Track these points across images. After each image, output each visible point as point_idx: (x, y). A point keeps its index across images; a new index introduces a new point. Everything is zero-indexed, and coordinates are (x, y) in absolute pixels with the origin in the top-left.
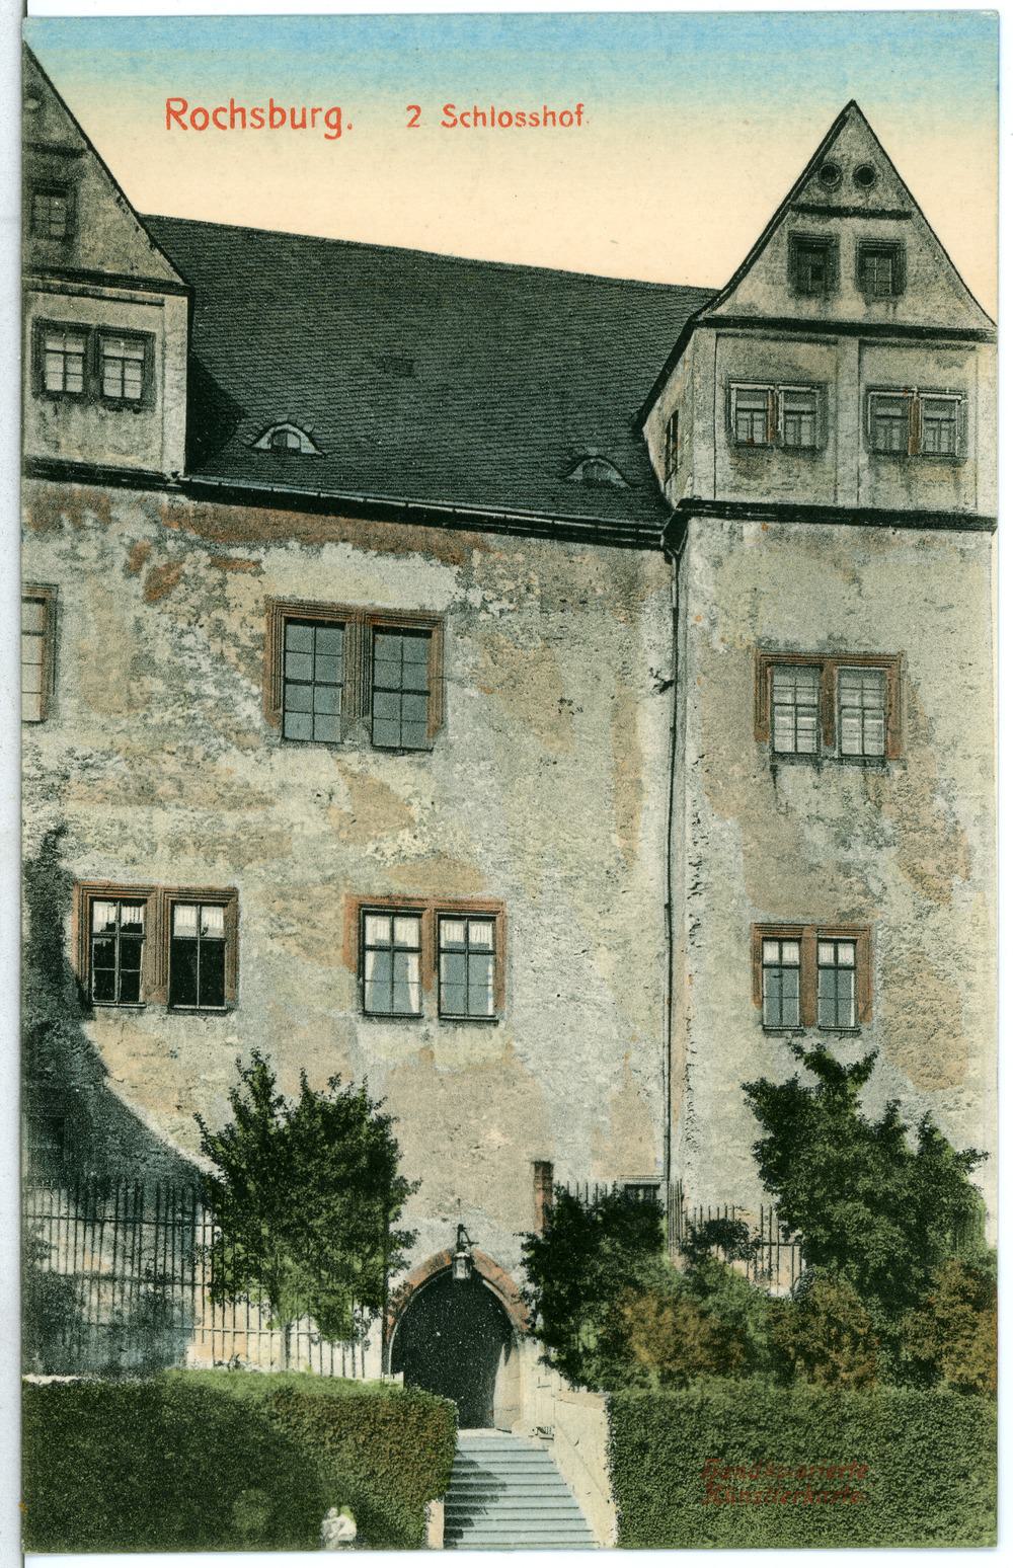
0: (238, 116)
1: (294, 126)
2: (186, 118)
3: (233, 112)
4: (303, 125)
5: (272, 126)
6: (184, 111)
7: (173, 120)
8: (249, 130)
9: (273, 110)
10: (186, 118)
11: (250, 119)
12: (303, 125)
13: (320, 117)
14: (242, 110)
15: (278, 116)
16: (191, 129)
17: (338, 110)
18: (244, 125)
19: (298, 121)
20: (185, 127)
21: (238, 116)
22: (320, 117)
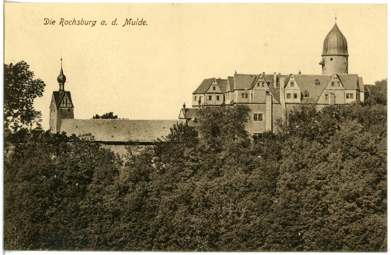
0: (75, 22)
2: (64, 23)
11: (77, 23)
13: (91, 23)
14: (75, 21)
17: (96, 22)
22: (91, 23)
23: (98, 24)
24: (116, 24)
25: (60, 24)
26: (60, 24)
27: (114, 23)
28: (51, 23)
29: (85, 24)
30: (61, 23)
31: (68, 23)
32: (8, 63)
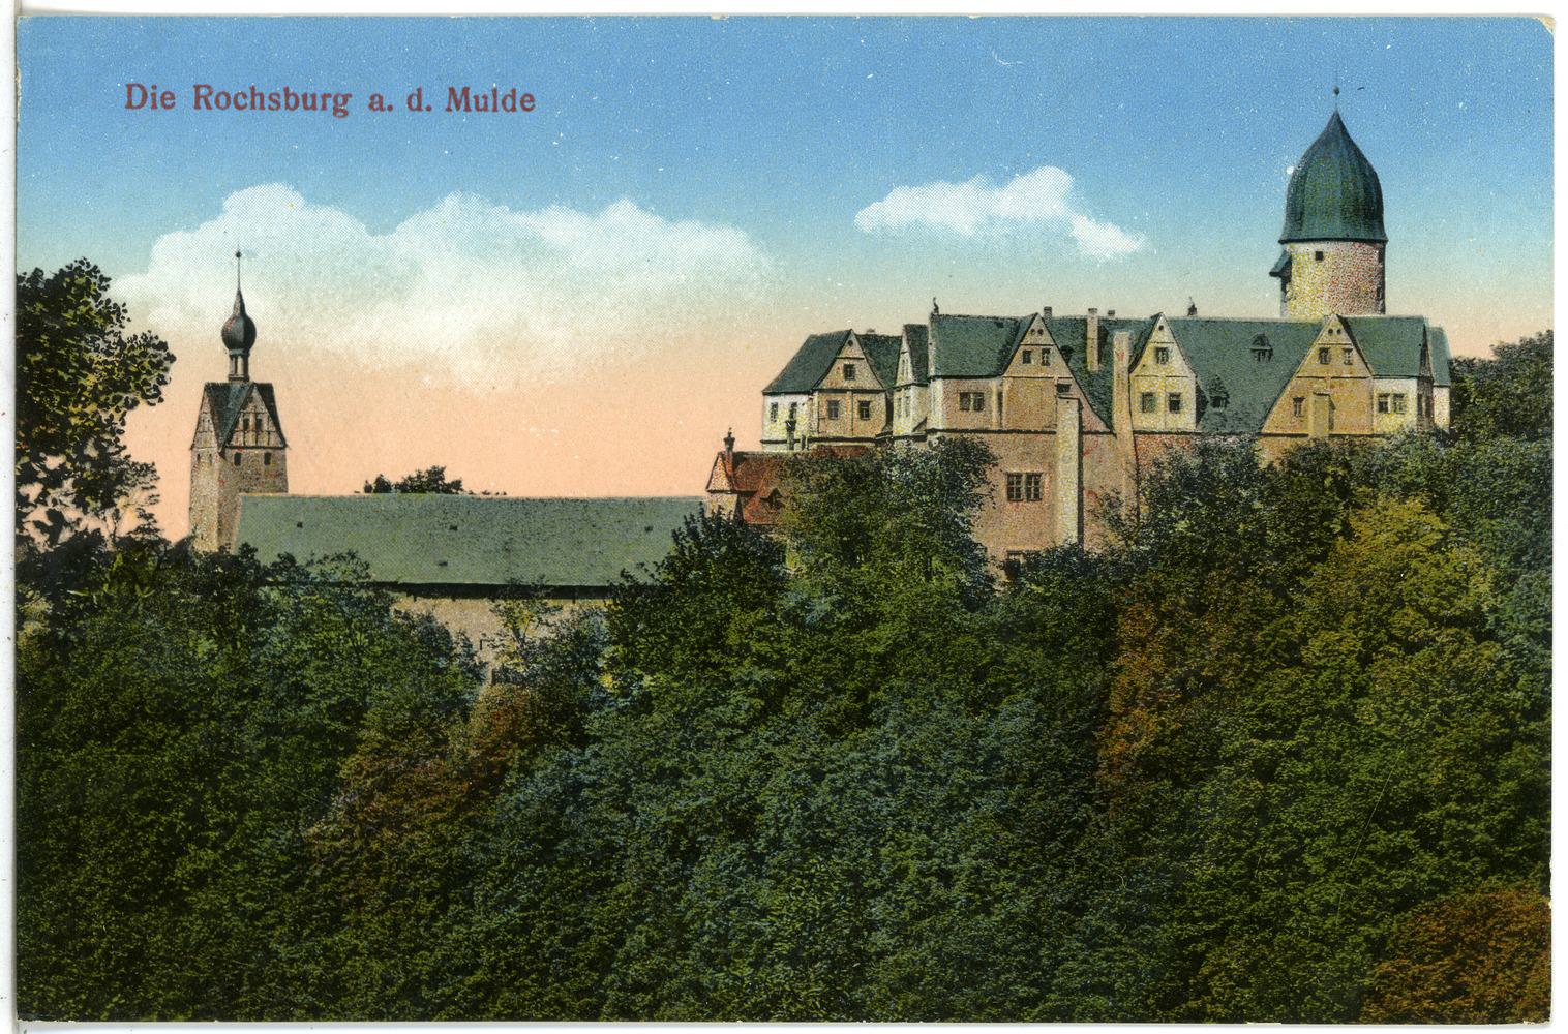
0: (257, 99)
1: (306, 108)
2: (212, 99)
3: (253, 95)
4: (314, 107)
5: (287, 106)
6: (210, 93)
7: (202, 101)
8: (266, 111)
9: (287, 95)
10: (212, 99)
12: (314, 107)
13: (330, 103)
14: (261, 95)
15: (292, 101)
16: (215, 109)
17: (346, 98)
18: (262, 107)
19: (310, 103)
20: (209, 107)
21: (257, 99)
22: (330, 103)
23: (358, 106)
24: (424, 106)
25: (197, 107)
26: (197, 107)
27: (416, 102)
28: (159, 105)
29: (306, 108)
30: (202, 101)
31: (232, 101)
32: (19, 273)
